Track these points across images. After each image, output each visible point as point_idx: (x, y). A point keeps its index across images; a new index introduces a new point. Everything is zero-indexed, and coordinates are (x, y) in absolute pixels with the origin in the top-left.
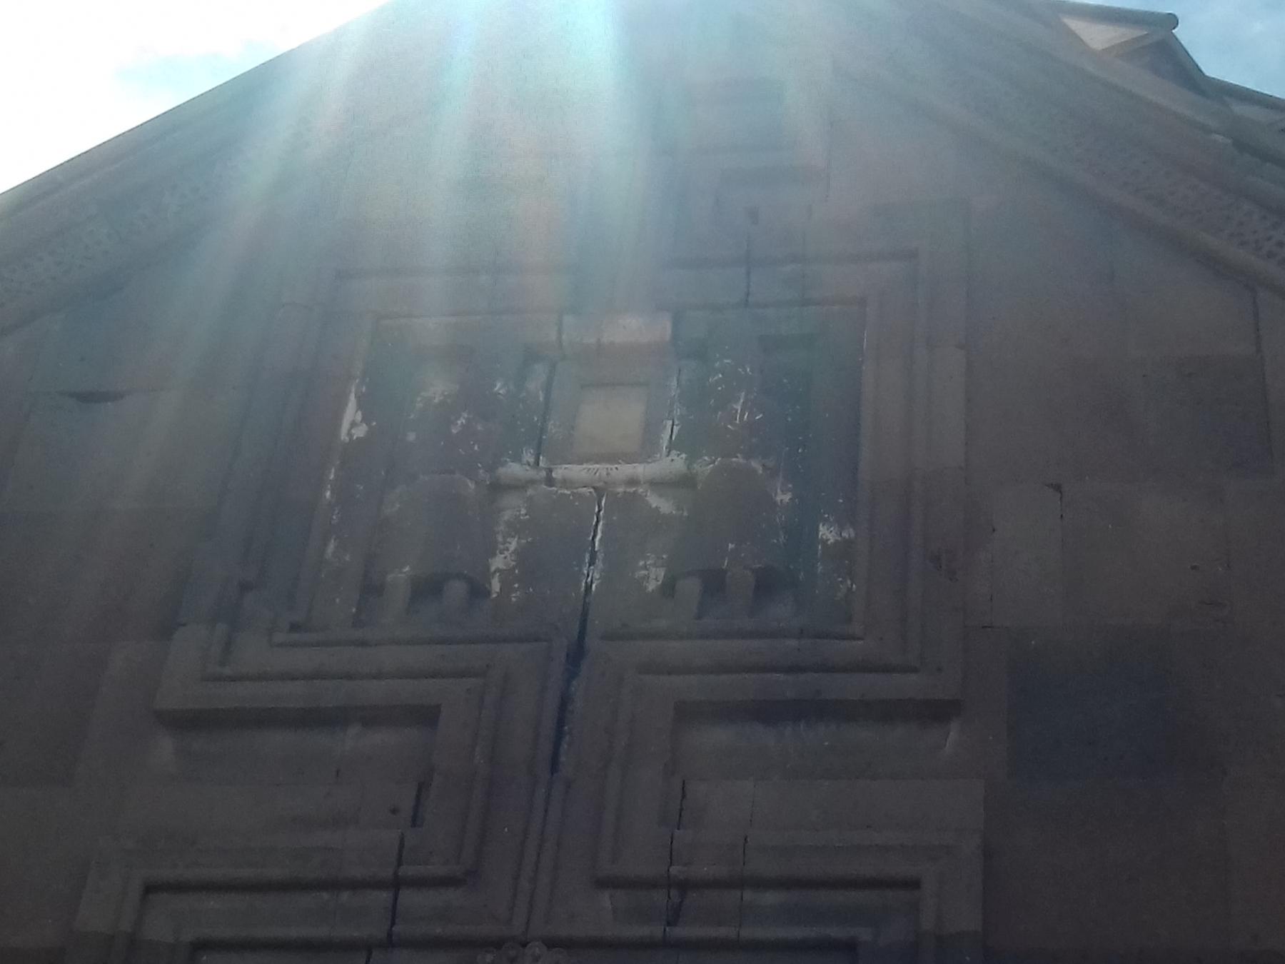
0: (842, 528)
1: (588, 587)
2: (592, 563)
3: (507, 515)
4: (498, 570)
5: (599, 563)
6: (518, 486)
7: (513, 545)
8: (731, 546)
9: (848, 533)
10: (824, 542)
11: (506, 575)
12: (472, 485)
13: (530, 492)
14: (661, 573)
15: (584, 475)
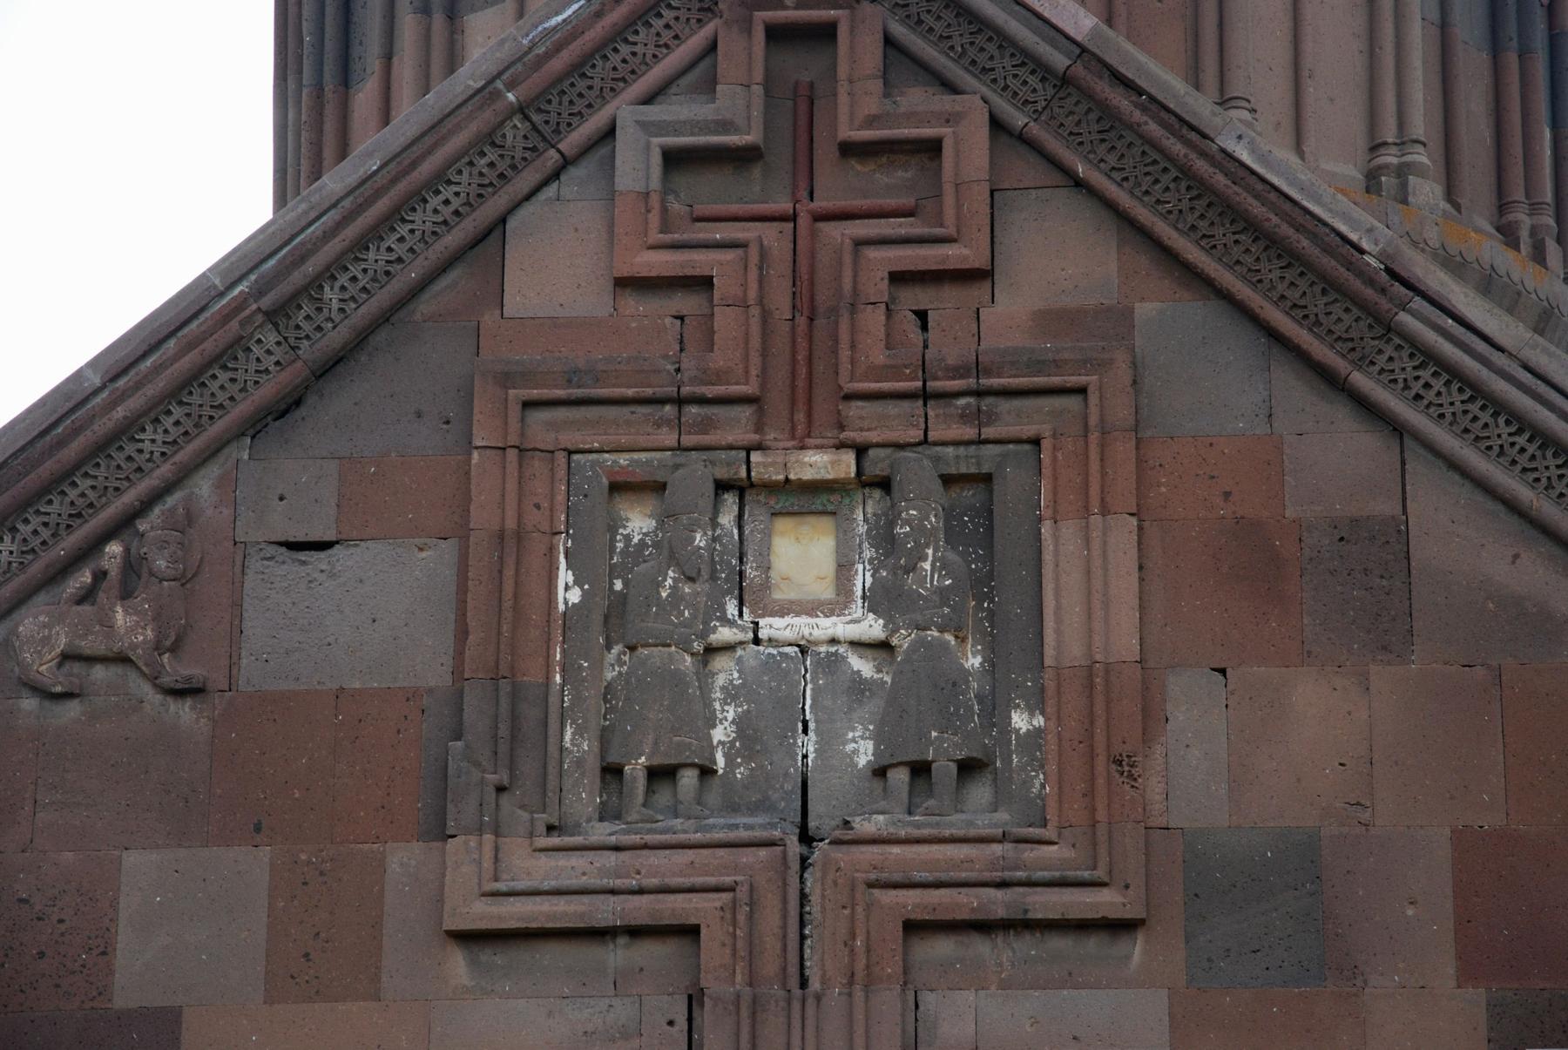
0: (1032, 715)
1: (805, 756)
2: (805, 731)
3: (721, 680)
4: (720, 742)
5: (811, 734)
6: (729, 648)
7: (731, 716)
8: (934, 734)
9: (1039, 721)
10: (1017, 731)
11: (729, 747)
12: (688, 658)
13: (739, 652)
14: (870, 745)
15: (788, 635)
